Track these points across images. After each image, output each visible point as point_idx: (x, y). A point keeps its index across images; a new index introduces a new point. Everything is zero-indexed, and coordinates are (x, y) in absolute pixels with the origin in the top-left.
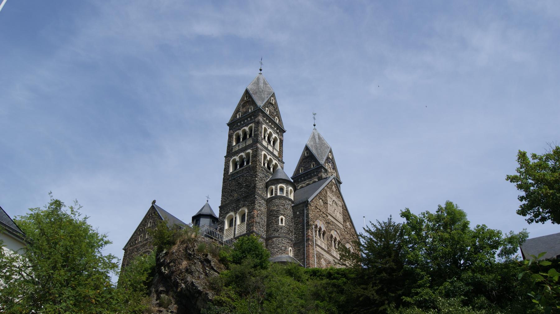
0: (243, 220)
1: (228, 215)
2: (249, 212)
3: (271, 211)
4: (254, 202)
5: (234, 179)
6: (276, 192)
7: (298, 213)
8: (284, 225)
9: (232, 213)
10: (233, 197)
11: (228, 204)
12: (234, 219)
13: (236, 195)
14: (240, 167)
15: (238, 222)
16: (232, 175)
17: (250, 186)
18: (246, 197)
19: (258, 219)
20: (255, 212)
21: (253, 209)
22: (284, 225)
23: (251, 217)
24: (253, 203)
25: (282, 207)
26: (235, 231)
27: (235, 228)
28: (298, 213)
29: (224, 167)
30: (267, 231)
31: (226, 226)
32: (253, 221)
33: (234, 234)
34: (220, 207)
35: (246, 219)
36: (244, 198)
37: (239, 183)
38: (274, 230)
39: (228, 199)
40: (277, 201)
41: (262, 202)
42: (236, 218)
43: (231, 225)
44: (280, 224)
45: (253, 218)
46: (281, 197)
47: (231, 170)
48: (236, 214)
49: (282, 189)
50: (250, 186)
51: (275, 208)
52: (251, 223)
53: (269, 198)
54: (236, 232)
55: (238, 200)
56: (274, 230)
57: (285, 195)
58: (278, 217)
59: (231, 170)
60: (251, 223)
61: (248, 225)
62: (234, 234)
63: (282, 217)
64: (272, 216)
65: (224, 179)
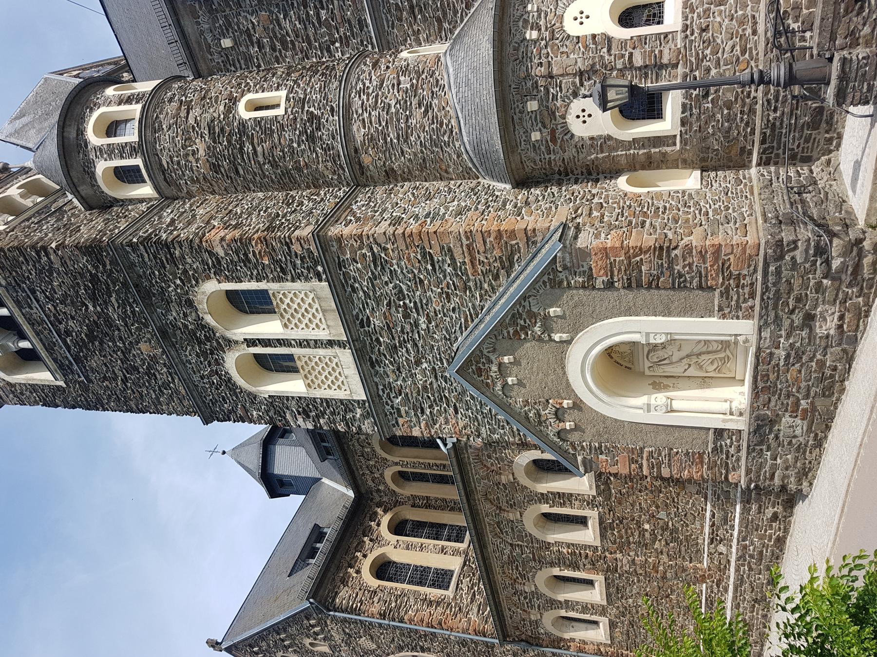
0: (257, 304)
1: (240, 381)
2: (218, 269)
3: (215, 168)
4: (167, 246)
5: (77, 359)
6: (122, 151)
7: (227, 43)
8: (283, 93)
9: (231, 361)
10: (154, 358)
11: (188, 382)
12: (259, 350)
13: (144, 346)
14: (23, 336)
15: (268, 327)
16: (63, 369)
17: (94, 279)
18: (146, 296)
19: (255, 225)
20: (218, 236)
21: (197, 247)
22: (283, 93)
23: (240, 258)
24: (164, 250)
25: (196, 112)
26: (317, 344)
27: (303, 343)
28: (227, 43)
29: (39, 408)
30: (316, 182)
31: (292, 386)
32: (264, 240)
33: (330, 343)
34: (207, 421)
35: (253, 285)
36: (149, 306)
37: (91, 337)
38: (311, 138)
39: (166, 385)
40: (166, 141)
41: (168, 216)
42: (251, 342)
43: (283, 365)
44: (280, 111)
45: (244, 243)
46: (148, 123)
47: (43, 376)
48: (230, 343)
49: (113, 128)
50: (94, 279)
51: (201, 147)
52: (271, 252)
53: (156, 188)
54: (323, 335)
55: (165, 334)
56: (311, 138)
57: (136, 109)
58: (243, 124)
59: (43, 376)
60: (271, 252)
61: (282, 273)
62: (330, 343)
63: (241, 106)
64: (239, 161)
65: (88, 407)
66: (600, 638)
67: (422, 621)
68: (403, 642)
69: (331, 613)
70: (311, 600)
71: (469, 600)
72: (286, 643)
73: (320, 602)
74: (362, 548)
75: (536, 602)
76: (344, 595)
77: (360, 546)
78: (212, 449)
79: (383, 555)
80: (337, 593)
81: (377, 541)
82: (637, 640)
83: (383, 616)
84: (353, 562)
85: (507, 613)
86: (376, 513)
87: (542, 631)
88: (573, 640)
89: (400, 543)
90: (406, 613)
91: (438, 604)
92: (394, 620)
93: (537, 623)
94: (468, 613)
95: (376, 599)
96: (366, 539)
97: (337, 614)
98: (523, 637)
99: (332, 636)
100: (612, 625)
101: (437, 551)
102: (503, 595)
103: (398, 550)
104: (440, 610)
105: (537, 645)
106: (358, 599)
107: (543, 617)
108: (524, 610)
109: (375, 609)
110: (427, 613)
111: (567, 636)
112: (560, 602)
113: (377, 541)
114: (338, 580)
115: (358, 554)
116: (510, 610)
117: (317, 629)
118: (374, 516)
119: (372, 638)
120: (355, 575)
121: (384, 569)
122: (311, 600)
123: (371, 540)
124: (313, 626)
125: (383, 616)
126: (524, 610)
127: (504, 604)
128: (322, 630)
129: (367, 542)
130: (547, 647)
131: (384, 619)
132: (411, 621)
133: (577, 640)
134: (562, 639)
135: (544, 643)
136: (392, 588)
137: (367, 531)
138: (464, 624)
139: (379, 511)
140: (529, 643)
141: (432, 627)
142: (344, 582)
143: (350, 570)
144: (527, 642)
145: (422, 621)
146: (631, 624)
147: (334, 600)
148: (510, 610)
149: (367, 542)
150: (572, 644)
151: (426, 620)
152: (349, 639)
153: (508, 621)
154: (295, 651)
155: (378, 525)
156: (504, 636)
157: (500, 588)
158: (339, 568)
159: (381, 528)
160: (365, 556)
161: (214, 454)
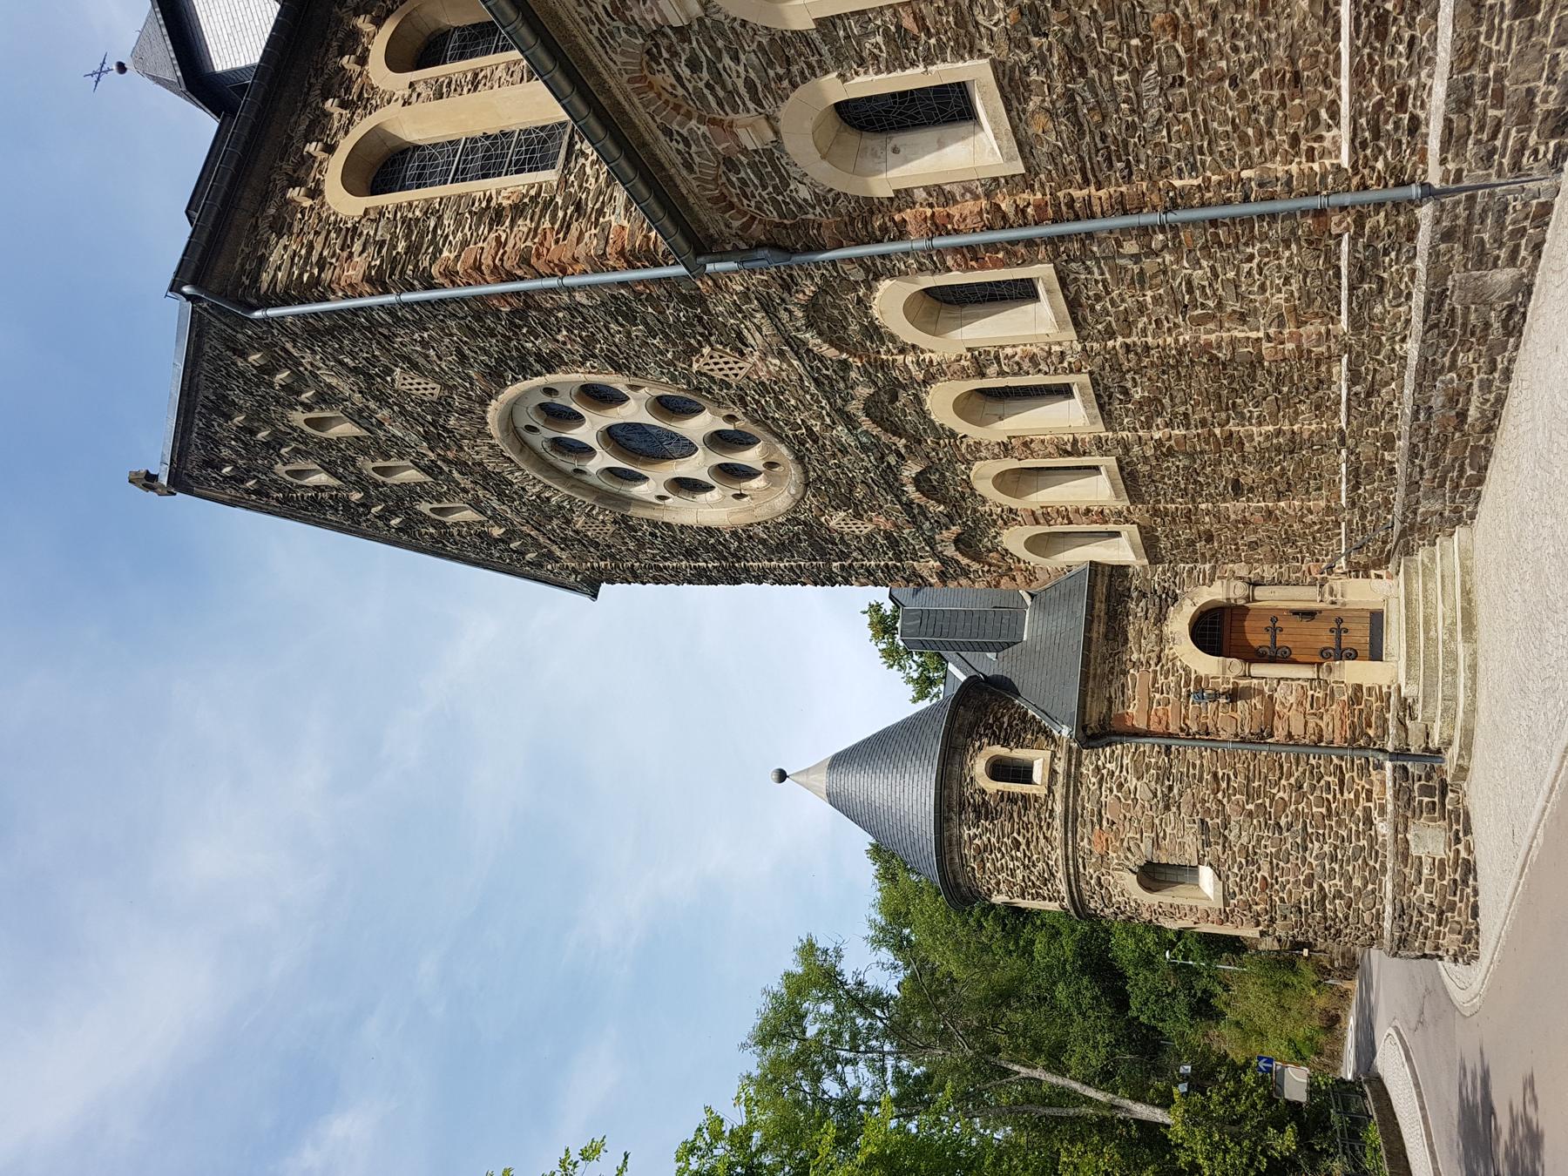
66: (991, 160)
67: (477, 267)
68: (486, 352)
69: (258, 314)
70: (186, 289)
71: (602, 177)
72: (263, 435)
73: (221, 295)
74: (323, 131)
75: (737, 73)
76: (280, 258)
77: (318, 126)
78: (97, 68)
79: (376, 131)
80: (263, 260)
81: (359, 102)
82: (1112, 130)
83: (377, 282)
84: (302, 173)
85: (667, 150)
86: (355, 34)
87: (804, 193)
88: (904, 197)
89: (420, 88)
90: (434, 259)
91: (518, 210)
92: (412, 289)
93: (771, 162)
94: (601, 212)
95: (357, 247)
96: (331, 105)
97: (271, 312)
98: (756, 230)
99: (330, 386)
100: (1012, 86)
101: (517, 77)
102: (616, 68)
103: (416, 107)
104: (524, 225)
105: (808, 249)
106: (314, 258)
107: (783, 127)
108: (713, 122)
109: (354, 272)
110: (489, 246)
111: (882, 185)
112: (802, 35)
113: (359, 102)
114: (263, 225)
115: (311, 148)
116: (668, 133)
117: (282, 376)
118: (353, 42)
119: (414, 366)
120: (307, 203)
121: (386, 166)
122: (186, 289)
123: (343, 105)
124: (268, 370)
125: (377, 282)
126: (713, 122)
127: (641, 116)
128: (298, 376)
129: (336, 111)
130: (841, 246)
131: (387, 292)
132: (451, 275)
133: (920, 195)
134: (871, 206)
135: (826, 234)
136: (399, 207)
137: (338, 85)
138: (591, 243)
139: (363, 23)
140: (785, 249)
141: (512, 277)
142: (281, 227)
143: (293, 193)
144: (774, 246)
145: (477, 267)
146: (1075, 60)
147: (256, 279)
148: (668, 133)
149: (336, 111)
150: (908, 214)
151: (487, 261)
152: (370, 379)
153: (687, 184)
154: (296, 451)
155: (362, 61)
156: (700, 245)
157: (587, 39)
158: (265, 198)
159: (369, 67)
160: (330, 149)
161: (104, 77)
